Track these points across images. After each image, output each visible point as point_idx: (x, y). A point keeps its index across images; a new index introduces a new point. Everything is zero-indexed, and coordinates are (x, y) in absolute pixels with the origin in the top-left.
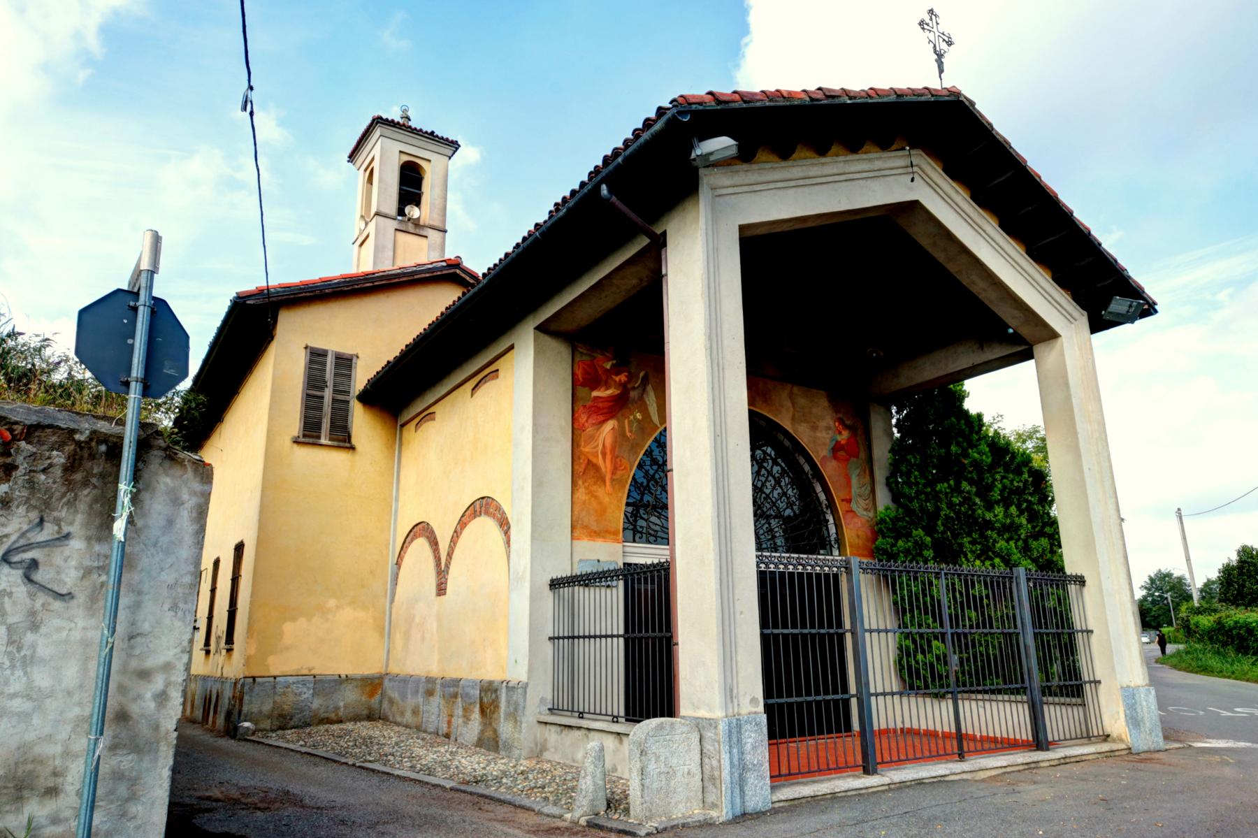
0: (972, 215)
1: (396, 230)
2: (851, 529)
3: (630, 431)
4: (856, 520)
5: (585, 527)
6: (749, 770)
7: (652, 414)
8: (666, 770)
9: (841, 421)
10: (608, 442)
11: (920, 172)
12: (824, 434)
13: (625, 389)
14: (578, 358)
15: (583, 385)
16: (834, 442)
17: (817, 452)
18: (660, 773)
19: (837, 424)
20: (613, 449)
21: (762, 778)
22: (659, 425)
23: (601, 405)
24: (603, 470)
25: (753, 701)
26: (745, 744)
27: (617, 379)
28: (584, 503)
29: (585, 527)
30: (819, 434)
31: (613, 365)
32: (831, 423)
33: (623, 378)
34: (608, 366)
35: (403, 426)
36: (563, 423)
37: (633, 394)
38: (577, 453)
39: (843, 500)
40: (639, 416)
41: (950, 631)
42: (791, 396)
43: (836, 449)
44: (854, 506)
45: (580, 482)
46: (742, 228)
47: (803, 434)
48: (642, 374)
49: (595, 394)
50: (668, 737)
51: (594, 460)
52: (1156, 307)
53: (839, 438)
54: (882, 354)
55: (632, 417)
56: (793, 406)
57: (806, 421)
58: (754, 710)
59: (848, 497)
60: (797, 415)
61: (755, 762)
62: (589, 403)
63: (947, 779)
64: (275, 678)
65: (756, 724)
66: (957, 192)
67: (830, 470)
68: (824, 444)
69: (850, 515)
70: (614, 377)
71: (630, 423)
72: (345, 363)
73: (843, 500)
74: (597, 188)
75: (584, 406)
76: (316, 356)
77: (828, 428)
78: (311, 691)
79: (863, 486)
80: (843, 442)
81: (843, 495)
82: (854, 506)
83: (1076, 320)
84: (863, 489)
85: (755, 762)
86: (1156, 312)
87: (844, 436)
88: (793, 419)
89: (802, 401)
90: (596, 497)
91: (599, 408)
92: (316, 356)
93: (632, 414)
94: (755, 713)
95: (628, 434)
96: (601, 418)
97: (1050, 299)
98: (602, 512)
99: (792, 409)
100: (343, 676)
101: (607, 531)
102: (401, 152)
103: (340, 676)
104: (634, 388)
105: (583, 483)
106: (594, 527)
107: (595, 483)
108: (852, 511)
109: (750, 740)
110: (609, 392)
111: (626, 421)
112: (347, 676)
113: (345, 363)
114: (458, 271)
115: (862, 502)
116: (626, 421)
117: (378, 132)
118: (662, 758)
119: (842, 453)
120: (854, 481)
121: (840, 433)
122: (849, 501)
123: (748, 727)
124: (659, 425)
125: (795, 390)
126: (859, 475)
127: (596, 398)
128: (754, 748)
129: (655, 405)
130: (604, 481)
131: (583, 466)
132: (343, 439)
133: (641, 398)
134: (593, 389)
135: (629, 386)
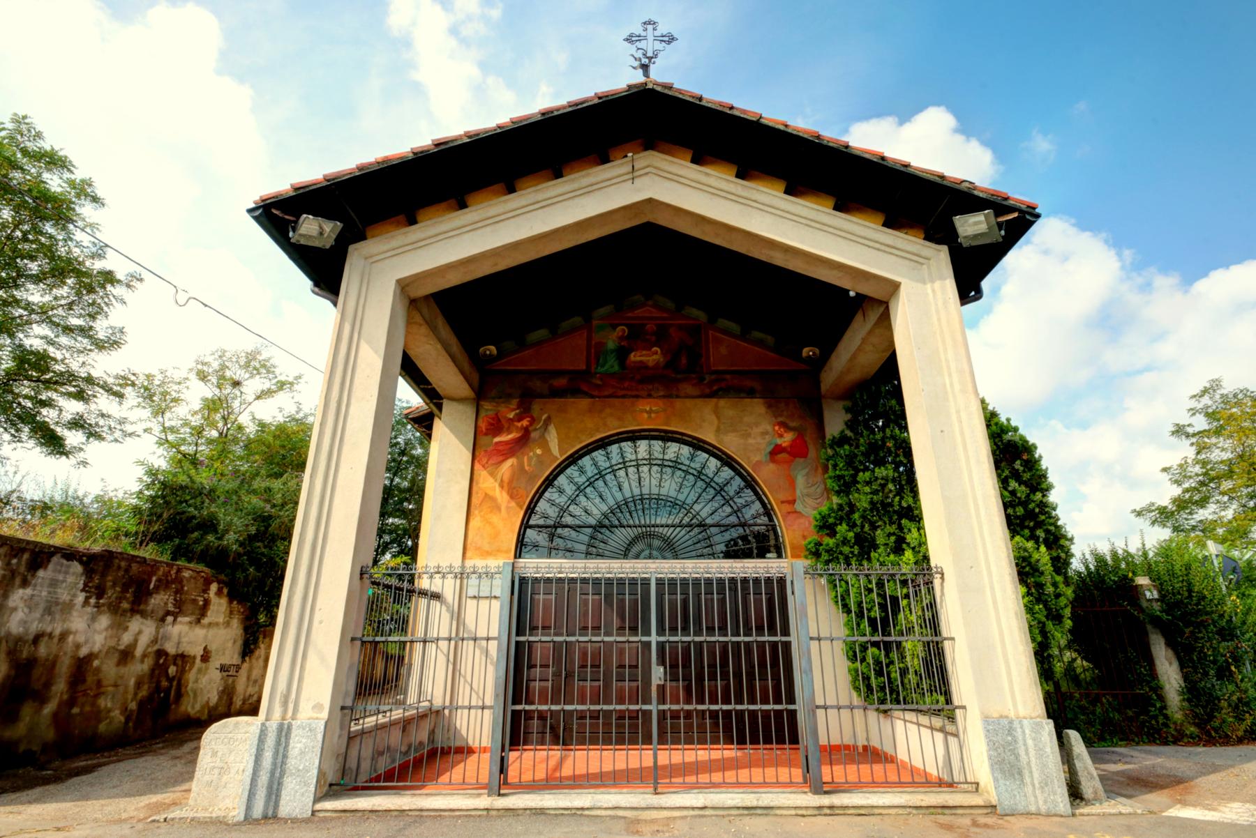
0: (733, 191)
2: (794, 530)
3: (529, 465)
4: (802, 521)
5: (478, 549)
6: (292, 774)
7: (552, 449)
8: (221, 765)
9: (782, 424)
10: (506, 479)
11: (654, 171)
12: (759, 440)
13: (526, 433)
14: (483, 414)
15: (486, 434)
16: (772, 447)
17: (749, 458)
18: (214, 767)
19: (777, 428)
20: (511, 482)
21: (306, 784)
22: (558, 456)
23: (501, 448)
24: (499, 500)
25: (317, 707)
26: (293, 748)
27: (519, 425)
28: (479, 528)
29: (478, 549)
30: (751, 441)
31: (516, 414)
32: (769, 428)
33: (525, 423)
34: (511, 415)
36: (463, 467)
37: (534, 435)
38: (475, 488)
39: (783, 502)
40: (539, 452)
42: (716, 412)
43: (776, 451)
44: (799, 506)
45: (477, 512)
46: (399, 281)
47: (731, 444)
48: (544, 417)
49: (497, 439)
50: (230, 735)
51: (491, 493)
52: (1037, 210)
53: (779, 441)
54: (817, 351)
55: (531, 454)
56: (718, 418)
57: (735, 431)
58: (315, 715)
59: (790, 498)
60: (722, 427)
61: (301, 768)
62: (491, 448)
63: (586, 812)
65: (310, 730)
66: (707, 174)
67: (766, 475)
68: (758, 449)
69: (792, 517)
70: (516, 424)
71: (530, 459)
73: (783, 502)
75: (486, 451)
77: (765, 433)
79: (813, 485)
80: (784, 445)
81: (782, 496)
82: (799, 506)
83: (928, 259)
84: (813, 488)
85: (301, 768)
87: (787, 439)
88: (718, 430)
89: (730, 413)
90: (490, 523)
91: (499, 451)
93: (532, 450)
94: (317, 718)
95: (527, 468)
96: (501, 458)
97: (877, 246)
98: (496, 535)
99: (716, 422)
101: (499, 551)
104: (536, 430)
105: (480, 512)
106: (486, 547)
107: (491, 512)
108: (796, 512)
109: (299, 745)
110: (510, 437)
111: (526, 458)
115: (810, 501)
116: (526, 458)
118: (219, 754)
119: (783, 456)
120: (800, 481)
121: (781, 436)
122: (793, 502)
123: (300, 732)
124: (558, 456)
125: (722, 402)
126: (807, 474)
127: (497, 443)
128: (302, 753)
129: (556, 440)
130: (499, 509)
131: (481, 499)
133: (542, 437)
134: (495, 435)
135: (530, 429)
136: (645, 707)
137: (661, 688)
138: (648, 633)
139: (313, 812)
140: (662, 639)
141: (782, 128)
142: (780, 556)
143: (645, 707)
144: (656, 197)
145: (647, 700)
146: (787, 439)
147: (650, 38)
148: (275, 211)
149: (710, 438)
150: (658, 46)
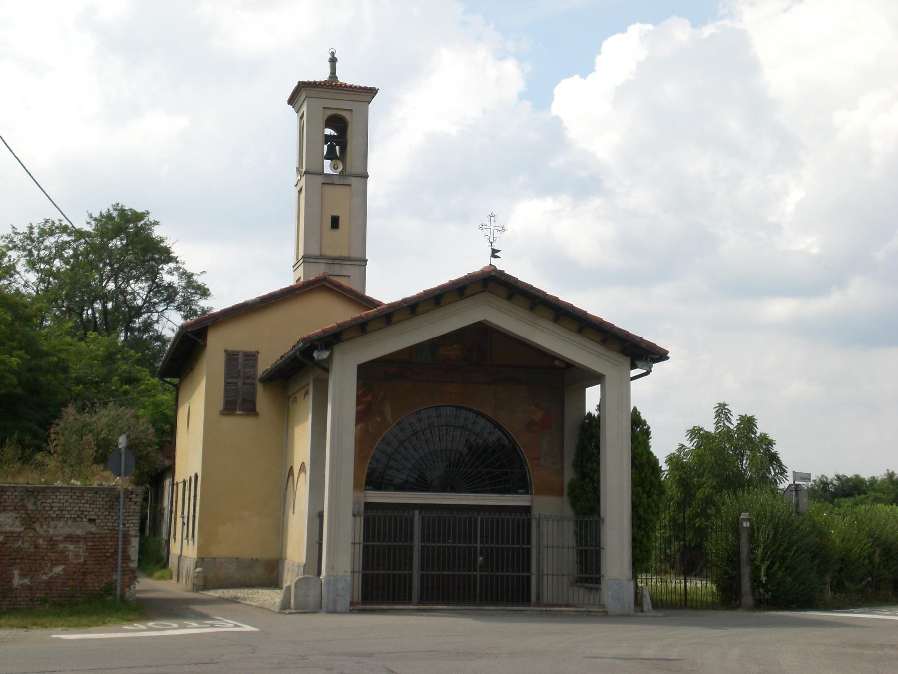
1: (323, 184)
19: (533, 408)
27: (365, 399)
33: (369, 398)
35: (289, 398)
40: (378, 419)
41: (479, 545)
52: (668, 356)
64: (214, 558)
72: (252, 358)
74: (296, 352)
76: (231, 357)
78: (235, 567)
86: (668, 358)
92: (231, 357)
100: (255, 559)
102: (324, 108)
103: (252, 559)
112: (257, 559)
113: (252, 358)
114: (325, 283)
117: (303, 96)
132: (251, 409)
136: (475, 573)
137: (481, 566)
138: (476, 542)
139: (350, 610)
140: (482, 545)
141: (556, 302)
142: (527, 493)
143: (475, 573)
144: (487, 319)
145: (475, 570)
146: (539, 416)
147: (492, 227)
148: (315, 343)
149: (490, 414)
150: (497, 234)
